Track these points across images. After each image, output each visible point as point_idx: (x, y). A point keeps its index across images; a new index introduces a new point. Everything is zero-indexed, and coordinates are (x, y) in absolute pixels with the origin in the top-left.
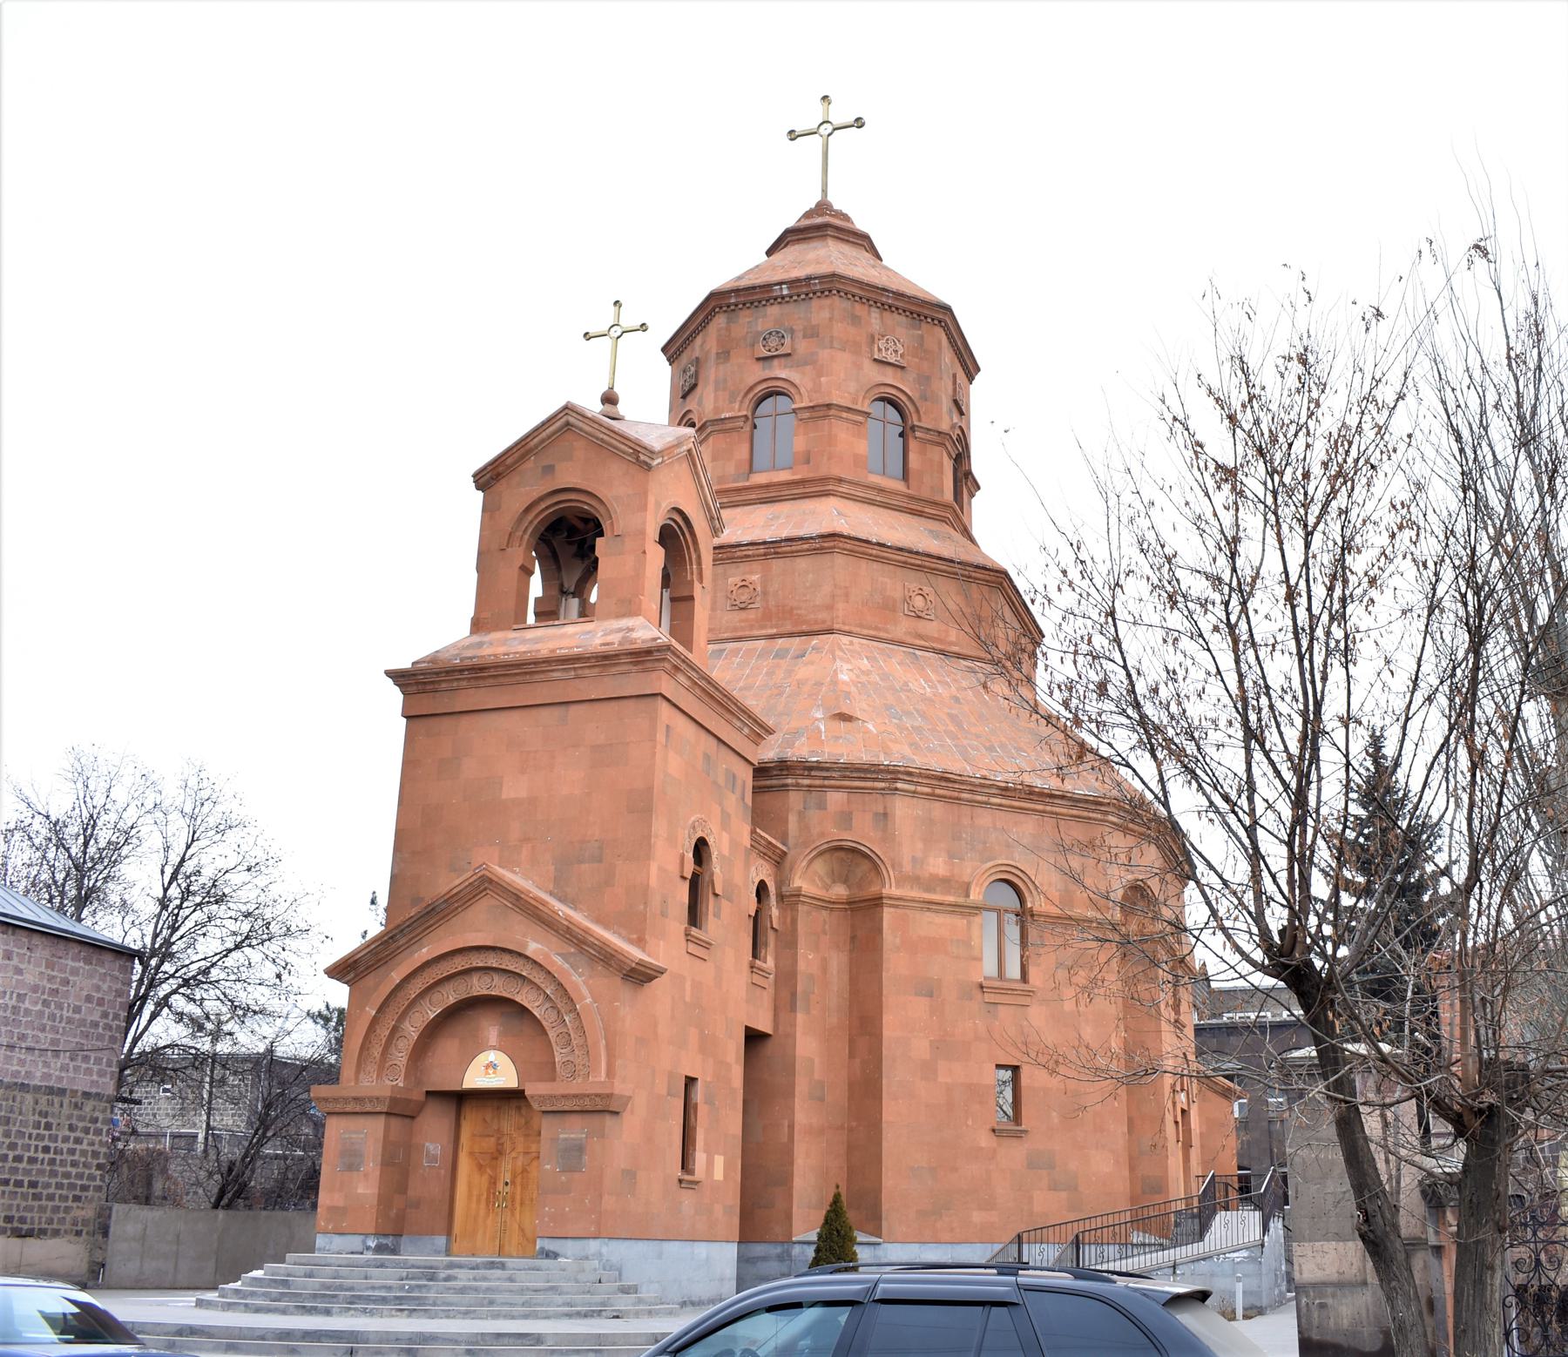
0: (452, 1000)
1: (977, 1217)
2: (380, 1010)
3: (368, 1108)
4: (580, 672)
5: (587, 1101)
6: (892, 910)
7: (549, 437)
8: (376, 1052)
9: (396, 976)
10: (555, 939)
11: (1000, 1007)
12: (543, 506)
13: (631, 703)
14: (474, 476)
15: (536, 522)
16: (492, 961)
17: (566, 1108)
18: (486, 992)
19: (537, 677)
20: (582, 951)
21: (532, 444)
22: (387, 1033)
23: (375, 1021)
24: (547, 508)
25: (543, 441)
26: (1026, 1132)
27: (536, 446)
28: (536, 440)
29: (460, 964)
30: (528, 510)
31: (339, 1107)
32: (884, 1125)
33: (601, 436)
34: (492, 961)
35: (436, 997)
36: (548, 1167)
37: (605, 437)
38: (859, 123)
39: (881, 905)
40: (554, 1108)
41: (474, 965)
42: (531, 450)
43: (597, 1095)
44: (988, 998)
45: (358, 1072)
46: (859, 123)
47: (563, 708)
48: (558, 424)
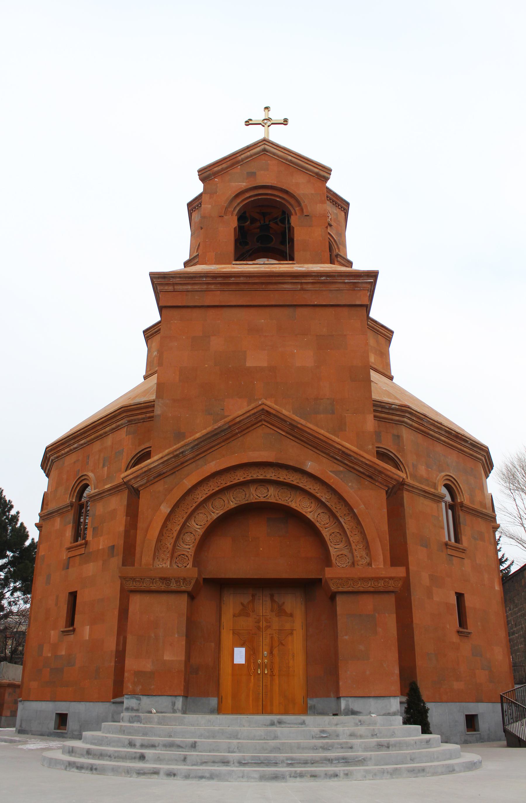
0: (233, 505)
1: (456, 685)
2: (172, 511)
3: (173, 586)
4: (305, 286)
5: (381, 584)
6: (407, 493)
7: (251, 156)
8: (169, 543)
9: (188, 483)
10: (325, 460)
11: (453, 557)
12: (247, 195)
13: (345, 310)
14: (199, 171)
15: (241, 205)
16: (271, 474)
17: (361, 589)
18: (263, 500)
19: (271, 287)
20: (351, 469)
21: (240, 158)
22: (178, 528)
23: (169, 518)
24: (250, 197)
25: (247, 158)
26: (469, 633)
27: (242, 160)
28: (243, 156)
29: (240, 477)
30: (237, 196)
31: (144, 586)
32: (414, 626)
33: (290, 158)
34: (271, 474)
35: (218, 503)
36: (346, 637)
37: (293, 159)
38: (285, 122)
39: (402, 490)
40: (350, 589)
41: (255, 477)
42: (238, 162)
43: (391, 578)
44: (450, 552)
45: (154, 559)
46: (285, 122)
47: (291, 310)
48: (258, 149)
